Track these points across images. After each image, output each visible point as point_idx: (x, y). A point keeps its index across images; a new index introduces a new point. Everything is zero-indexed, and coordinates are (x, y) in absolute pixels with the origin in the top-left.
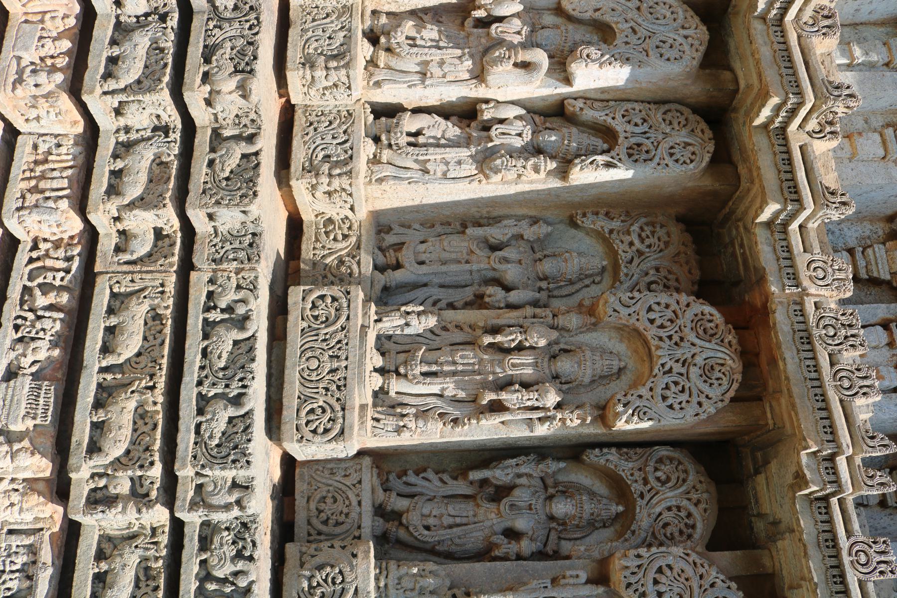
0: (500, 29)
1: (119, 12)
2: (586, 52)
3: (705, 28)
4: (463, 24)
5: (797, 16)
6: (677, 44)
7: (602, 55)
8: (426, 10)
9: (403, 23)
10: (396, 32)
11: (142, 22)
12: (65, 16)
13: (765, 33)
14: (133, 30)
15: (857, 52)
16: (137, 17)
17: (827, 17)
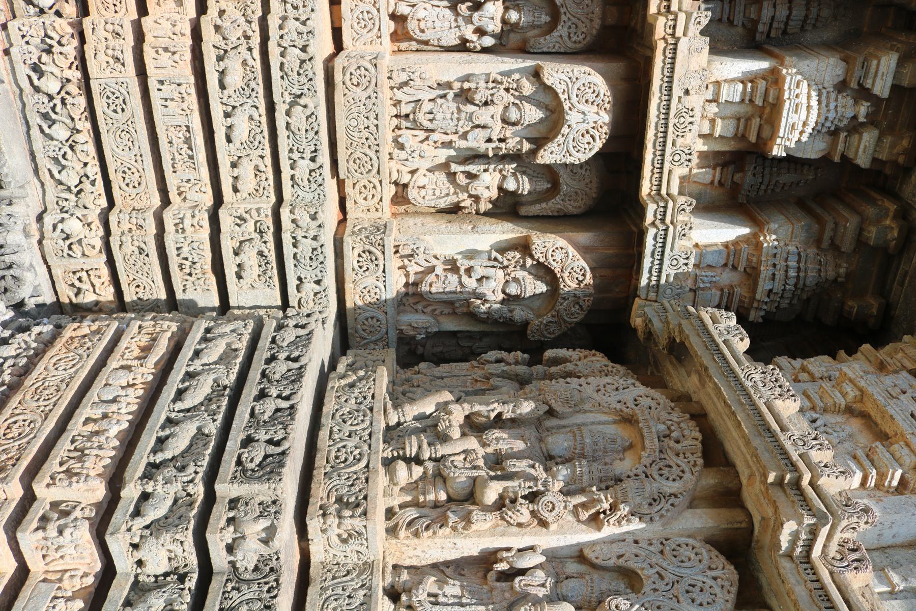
0: (523, 582)
1: (139, 571)
2: (614, 603)
3: (732, 567)
4: (485, 576)
5: (823, 551)
6: (708, 587)
7: (631, 605)
8: (447, 564)
9: (425, 580)
10: (417, 590)
11: (159, 582)
12: (85, 575)
13: (795, 571)
14: (150, 590)
15: (896, 579)
16: (156, 577)
17: (854, 550)
